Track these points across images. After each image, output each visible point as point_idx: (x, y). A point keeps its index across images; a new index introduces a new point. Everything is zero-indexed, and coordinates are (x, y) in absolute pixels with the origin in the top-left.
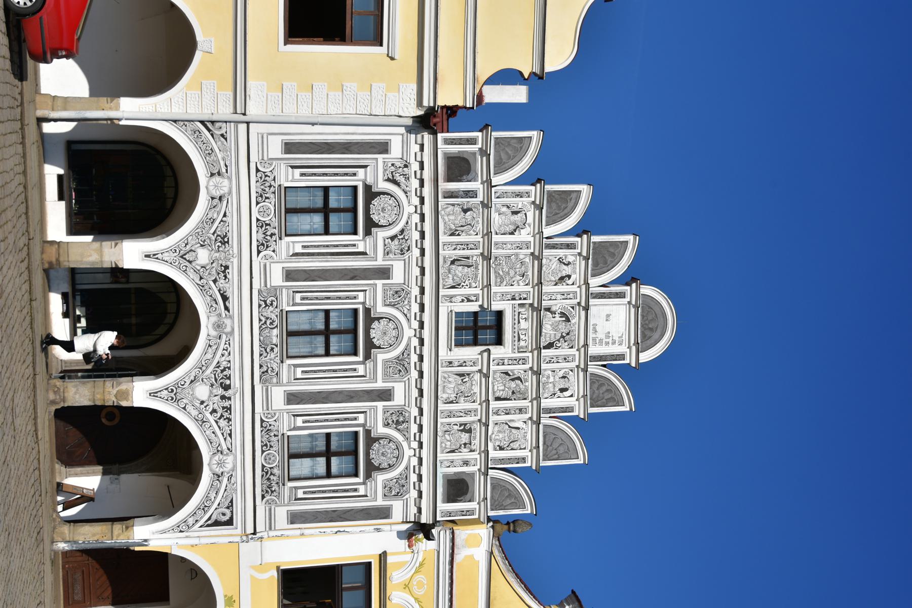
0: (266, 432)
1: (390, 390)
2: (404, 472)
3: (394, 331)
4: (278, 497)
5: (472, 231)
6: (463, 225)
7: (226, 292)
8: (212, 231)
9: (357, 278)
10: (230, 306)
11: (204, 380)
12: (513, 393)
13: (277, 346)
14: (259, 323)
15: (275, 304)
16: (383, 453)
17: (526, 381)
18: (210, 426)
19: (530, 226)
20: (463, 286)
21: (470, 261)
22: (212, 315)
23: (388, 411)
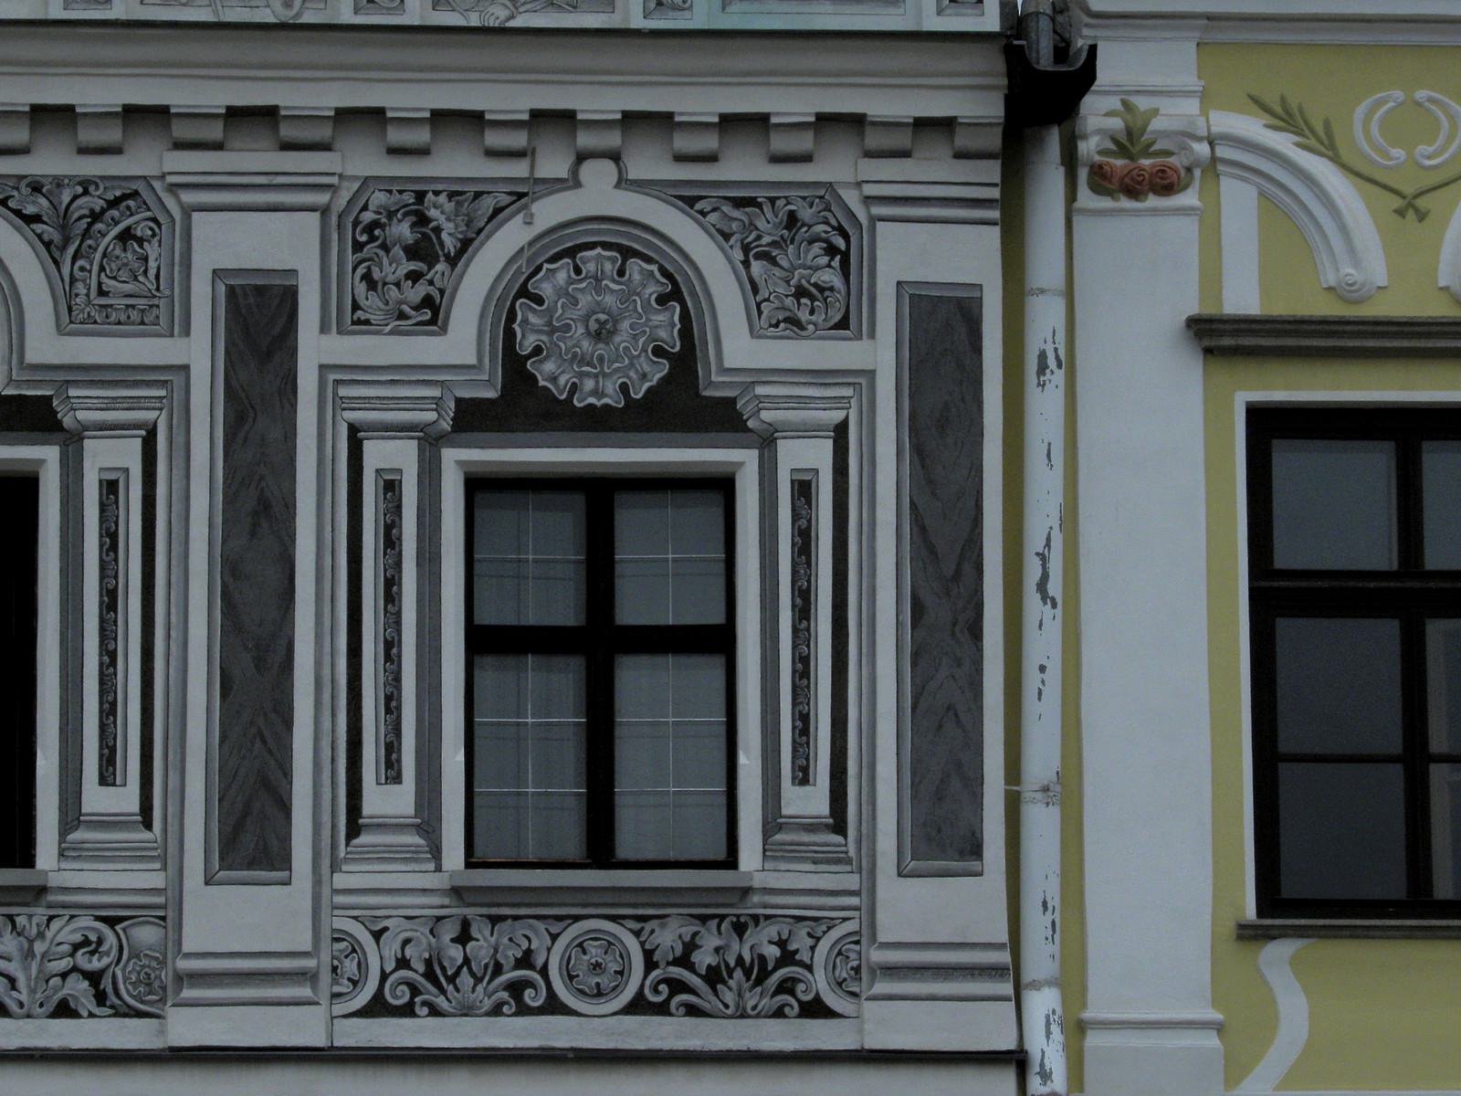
0: (443, 991)
1: (231, 291)
2: (713, 218)
4: (817, 925)
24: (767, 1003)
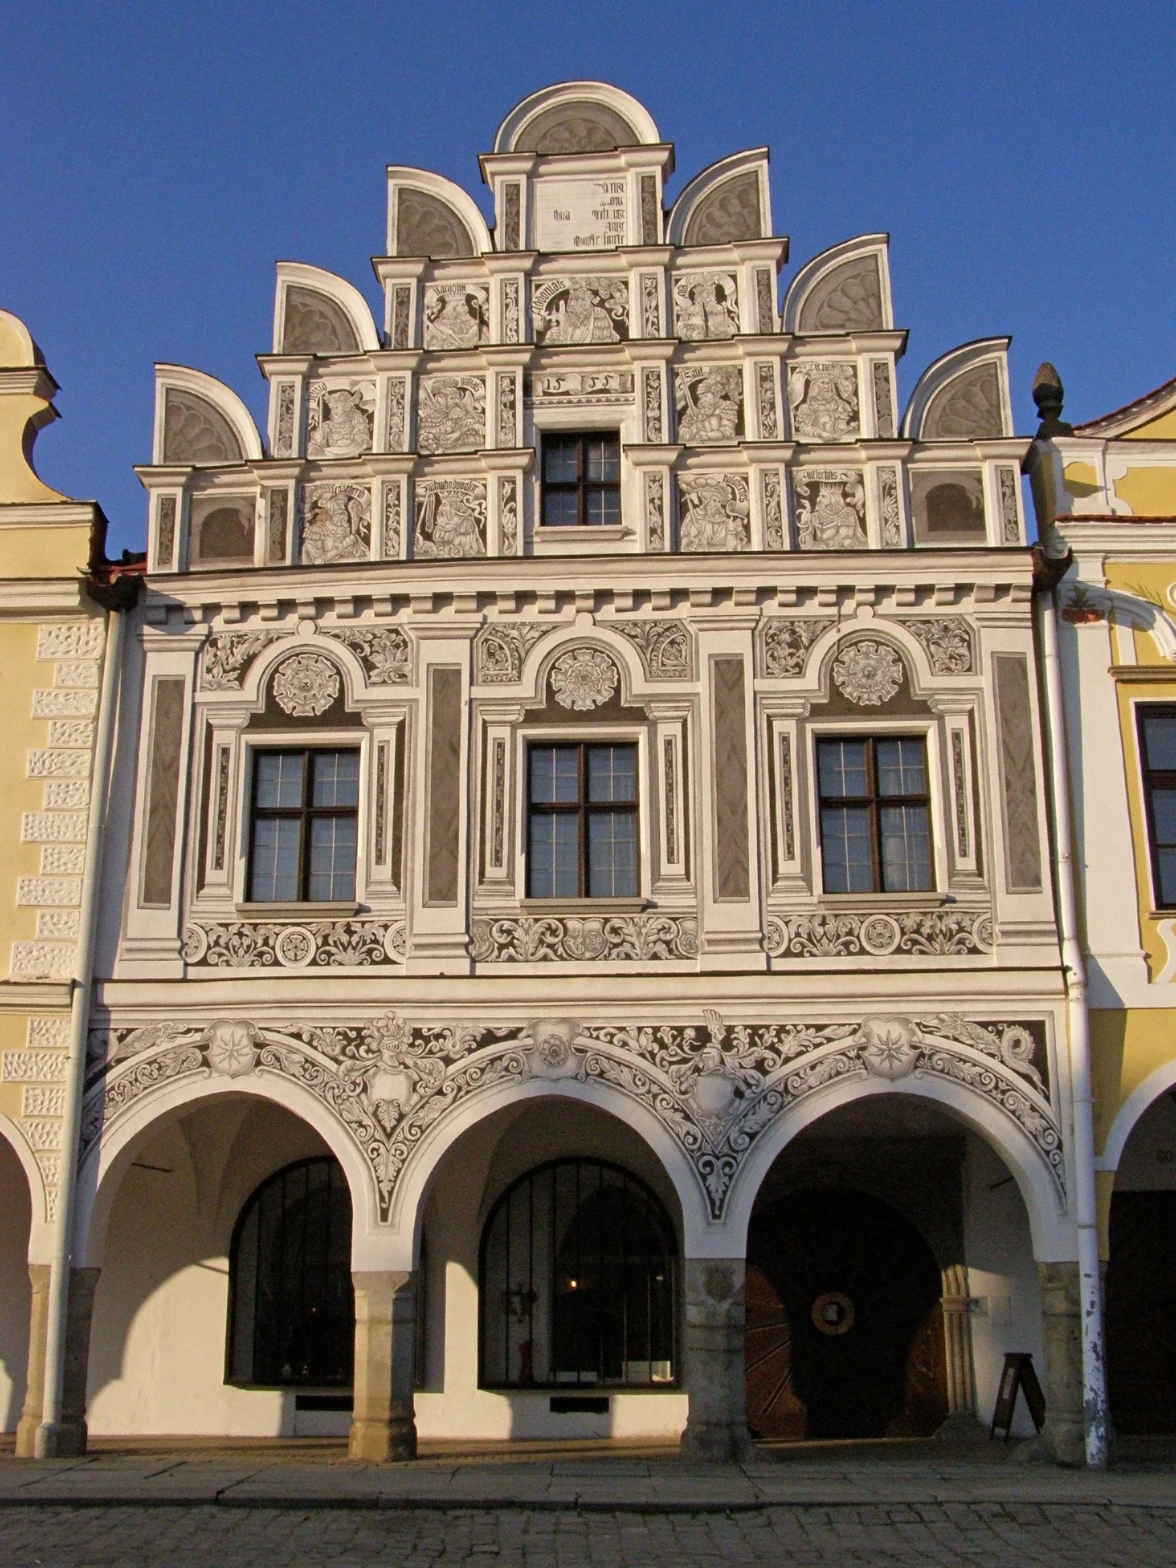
0: (815, 946)
1: (717, 663)
2: (913, 628)
3: (581, 659)
5: (362, 500)
6: (346, 518)
7: (475, 1037)
8: (332, 1066)
9: (454, 740)
10: (504, 1028)
11: (683, 1088)
12: (726, 397)
13: (607, 920)
14: (552, 960)
15: (507, 925)
16: (868, 677)
17: (698, 371)
18: (798, 1075)
19: (356, 383)
20: (481, 513)
21: (426, 500)
22: (527, 1068)
23: (768, 667)
24: (953, 948)
